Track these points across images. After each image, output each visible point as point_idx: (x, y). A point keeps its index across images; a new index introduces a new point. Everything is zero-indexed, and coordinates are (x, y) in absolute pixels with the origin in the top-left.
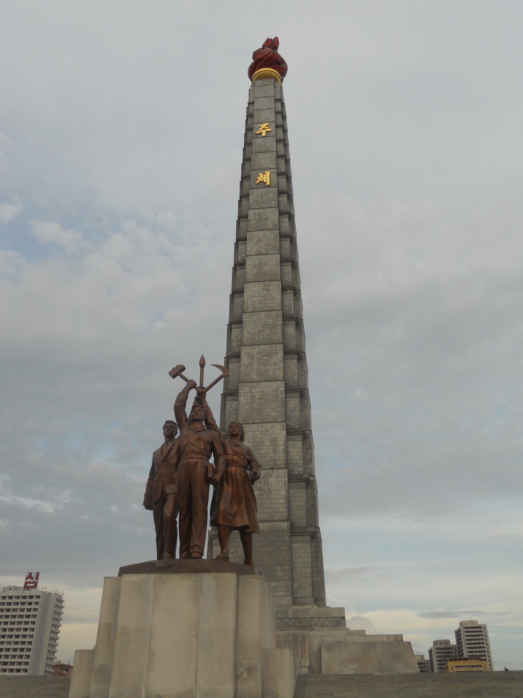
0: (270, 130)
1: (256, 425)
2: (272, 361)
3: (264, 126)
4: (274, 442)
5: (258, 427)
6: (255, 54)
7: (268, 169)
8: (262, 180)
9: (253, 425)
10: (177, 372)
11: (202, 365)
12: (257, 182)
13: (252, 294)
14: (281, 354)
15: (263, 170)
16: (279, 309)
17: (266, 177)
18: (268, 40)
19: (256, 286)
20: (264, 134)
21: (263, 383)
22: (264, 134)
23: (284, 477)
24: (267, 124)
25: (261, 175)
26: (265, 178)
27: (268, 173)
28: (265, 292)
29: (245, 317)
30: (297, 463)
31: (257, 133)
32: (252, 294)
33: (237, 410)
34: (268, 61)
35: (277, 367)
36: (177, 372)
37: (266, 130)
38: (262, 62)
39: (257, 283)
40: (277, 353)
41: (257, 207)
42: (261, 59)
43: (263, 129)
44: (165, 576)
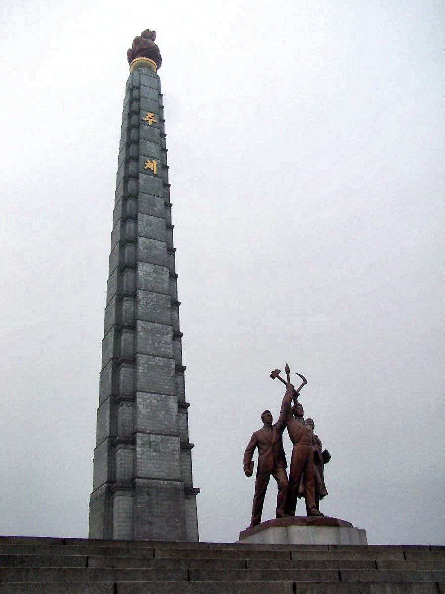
0: (155, 121)
1: (153, 395)
2: (164, 339)
3: (150, 115)
4: (168, 411)
5: (155, 396)
6: (137, 41)
7: (155, 159)
8: (150, 168)
9: (151, 394)
10: (275, 374)
11: (288, 371)
12: (146, 168)
13: (144, 273)
14: (170, 335)
15: (152, 158)
16: (166, 293)
17: (153, 165)
18: (148, 31)
19: (148, 267)
20: (150, 123)
21: (157, 358)
22: (150, 123)
23: (178, 444)
24: (153, 115)
25: (149, 162)
26: (152, 166)
27: (155, 163)
28: (155, 275)
29: (140, 293)
30: (183, 432)
31: (145, 119)
32: (144, 273)
33: (135, 377)
34: (145, 50)
35: (168, 346)
36: (275, 374)
37: (152, 120)
38: (146, 52)
39: (148, 264)
40: (167, 334)
41: (146, 191)
42: (146, 49)
43: (150, 118)
44: (319, 528)
